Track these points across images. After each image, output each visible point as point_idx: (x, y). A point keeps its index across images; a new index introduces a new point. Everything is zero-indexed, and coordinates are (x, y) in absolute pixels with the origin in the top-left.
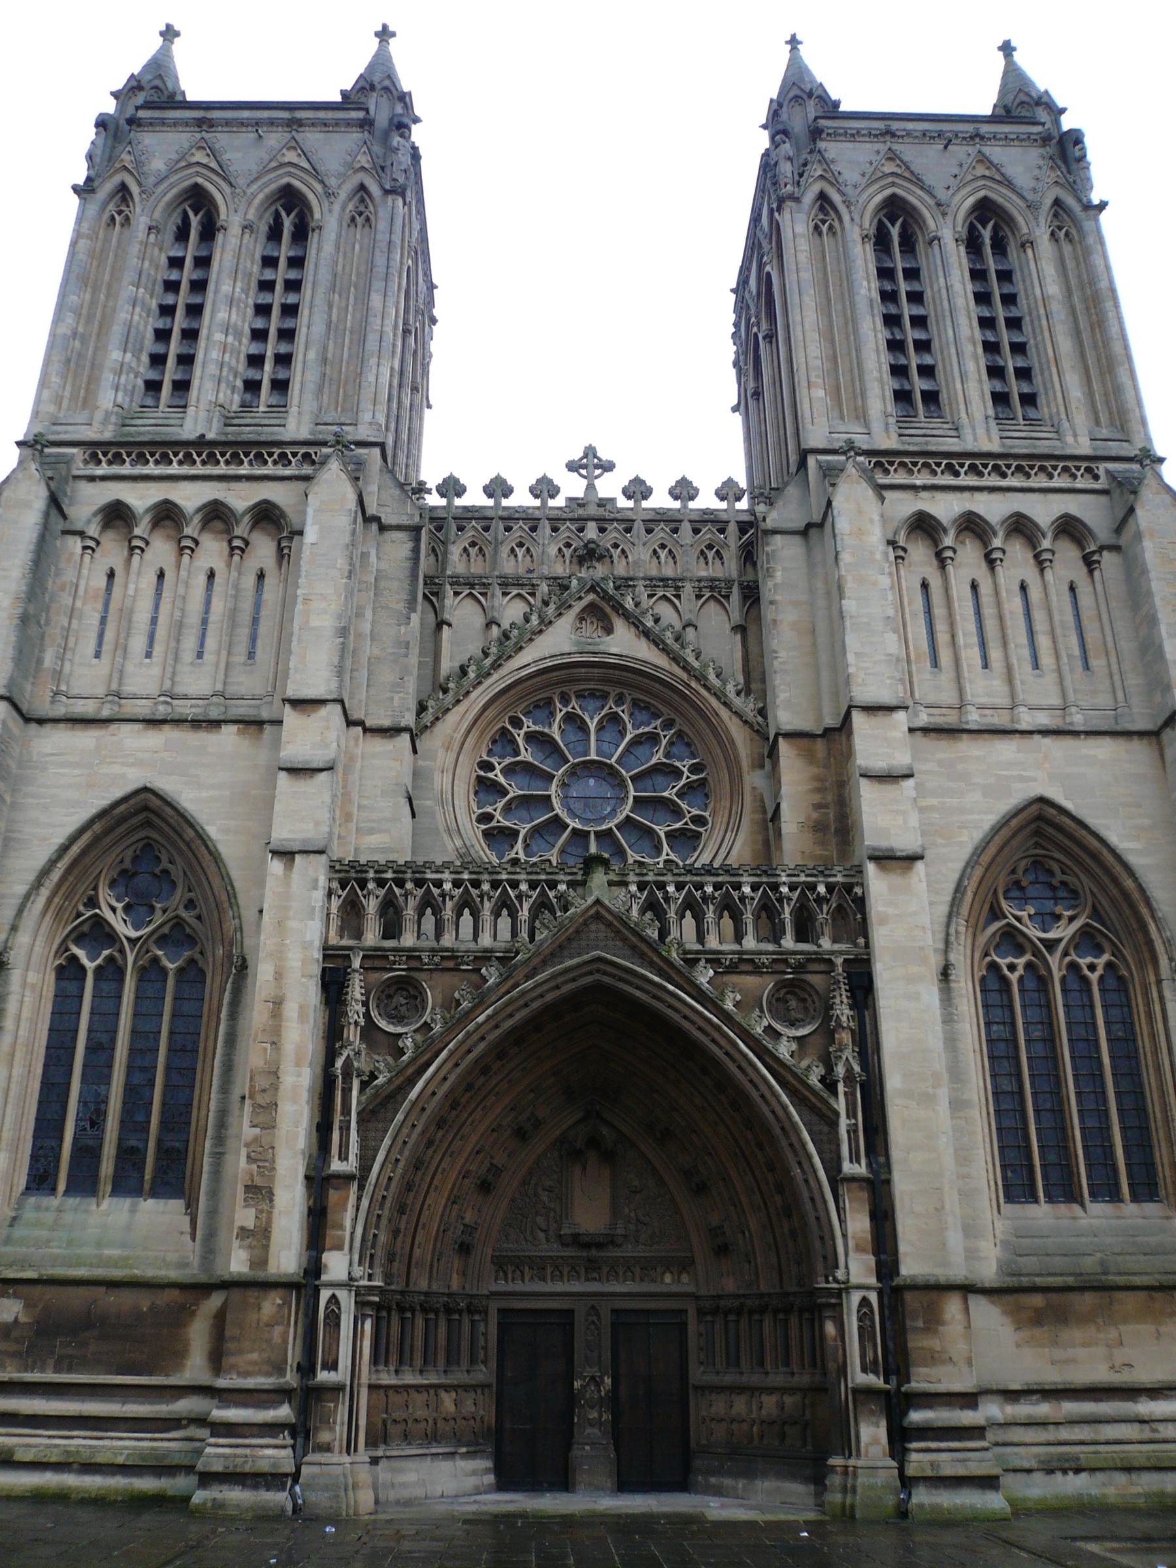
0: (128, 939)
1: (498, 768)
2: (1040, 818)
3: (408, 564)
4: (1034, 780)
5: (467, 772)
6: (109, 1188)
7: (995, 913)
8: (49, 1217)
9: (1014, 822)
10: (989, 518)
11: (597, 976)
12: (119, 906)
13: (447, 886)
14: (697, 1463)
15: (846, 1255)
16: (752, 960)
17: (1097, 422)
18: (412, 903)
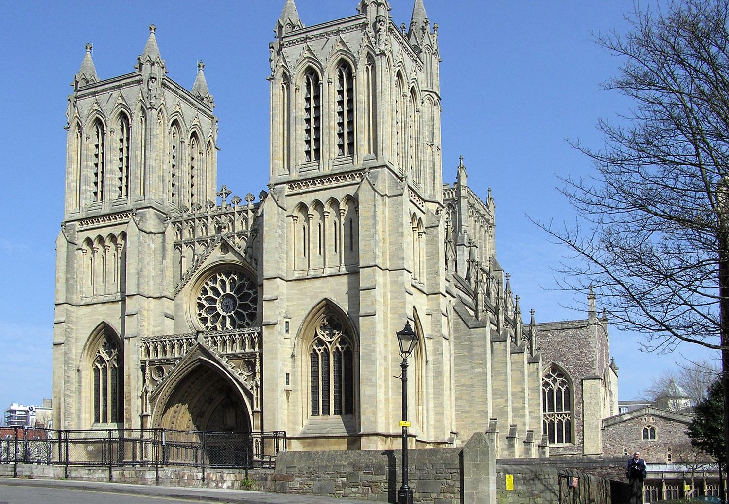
3: (162, 245)
4: (325, 292)
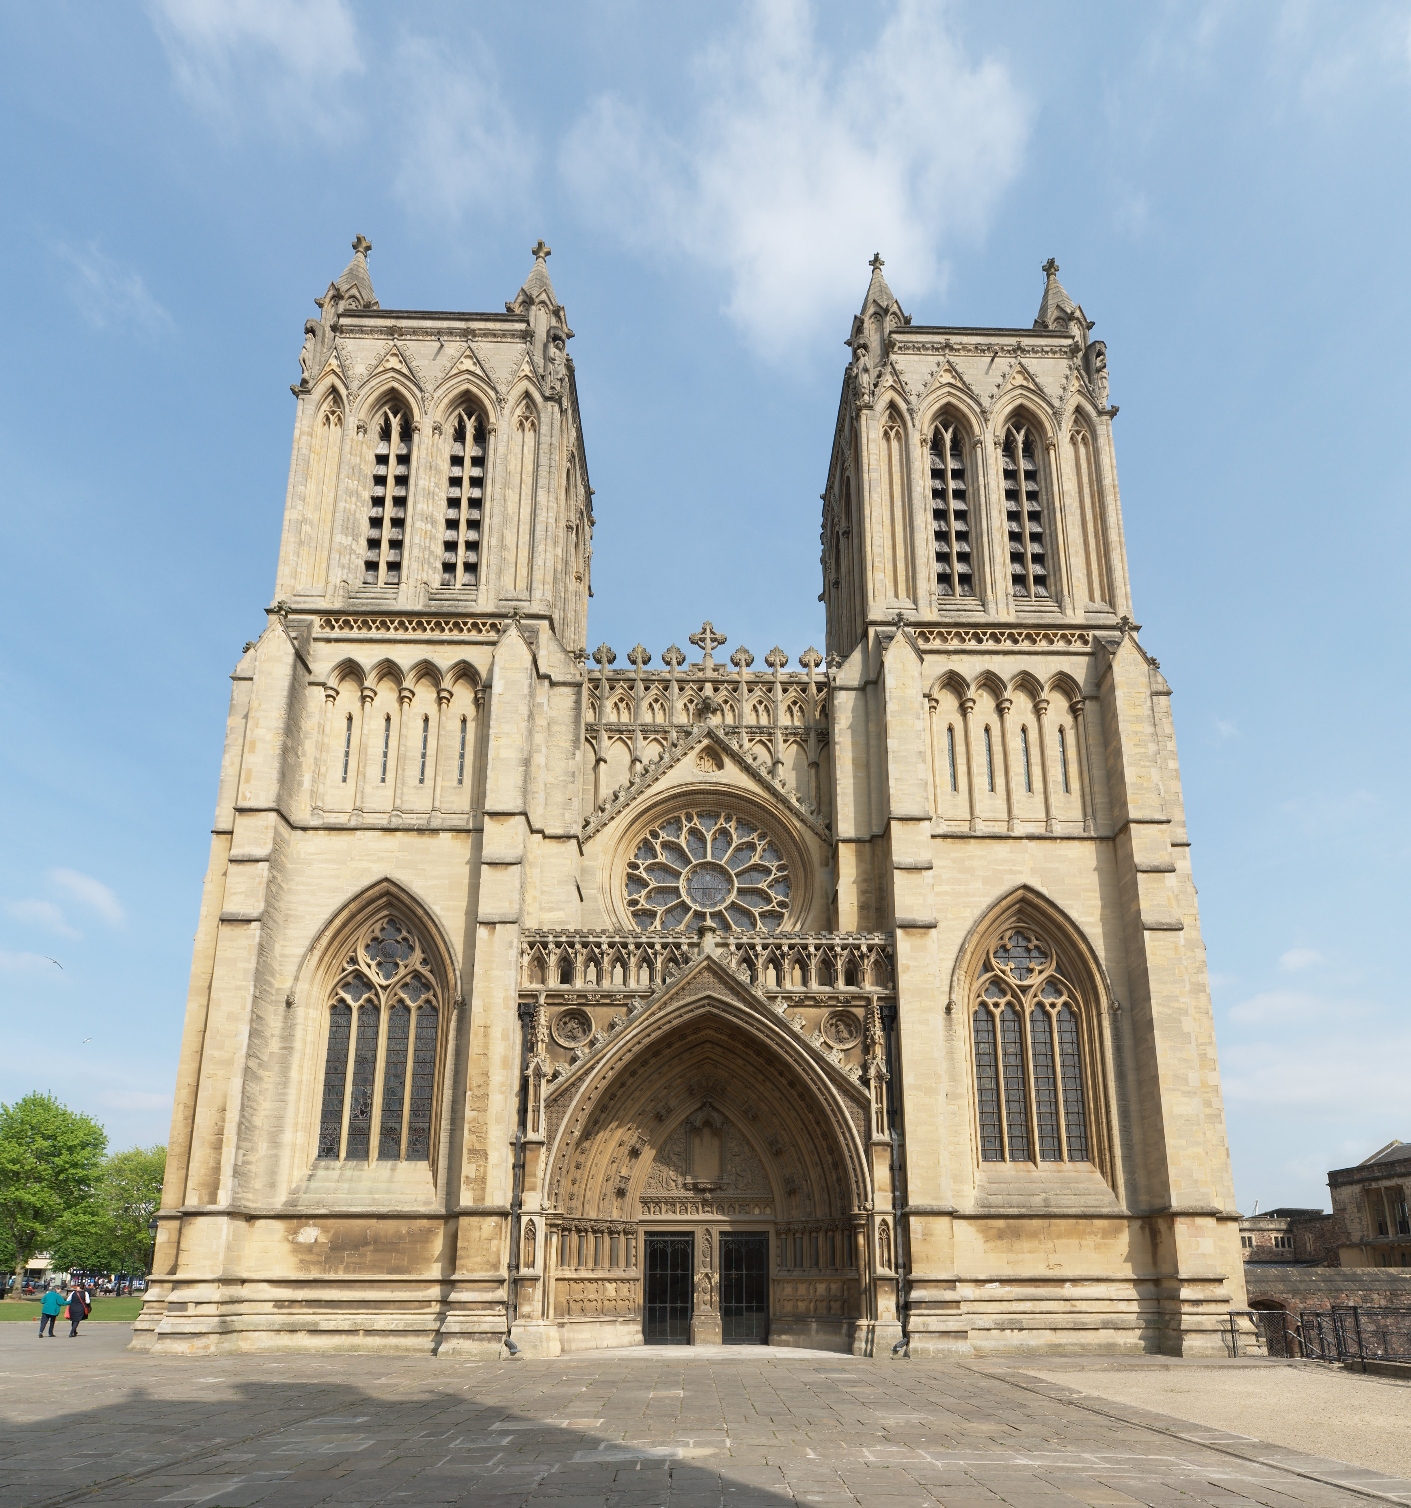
0: (381, 986)
1: (642, 867)
2: (1023, 900)
3: (572, 713)
4: (1021, 872)
5: (620, 871)
6: (376, 1155)
7: (987, 967)
8: (335, 1174)
9: (1004, 903)
10: (1001, 675)
11: (708, 1008)
12: (373, 964)
13: (605, 947)
14: (774, 1327)
15: (873, 1193)
16: (814, 998)
17: (1092, 599)
18: (580, 959)
